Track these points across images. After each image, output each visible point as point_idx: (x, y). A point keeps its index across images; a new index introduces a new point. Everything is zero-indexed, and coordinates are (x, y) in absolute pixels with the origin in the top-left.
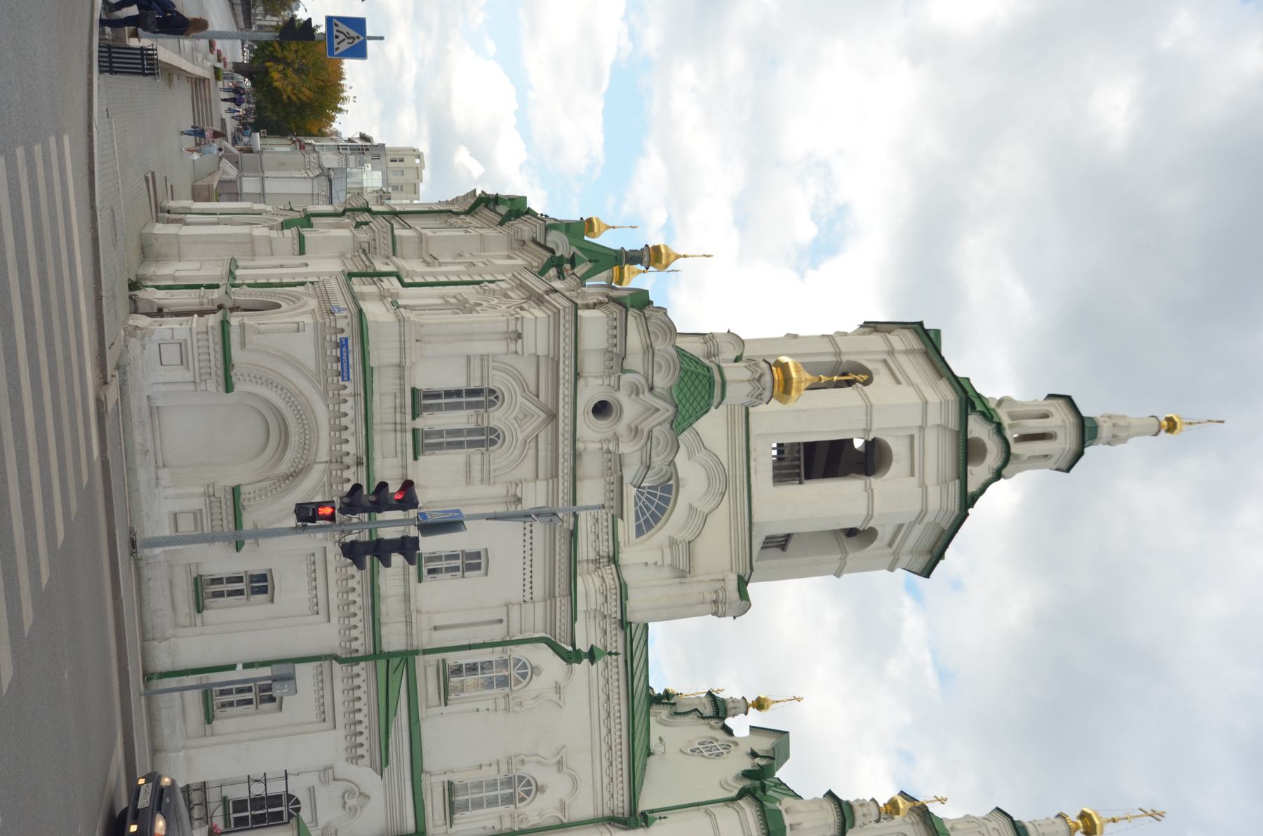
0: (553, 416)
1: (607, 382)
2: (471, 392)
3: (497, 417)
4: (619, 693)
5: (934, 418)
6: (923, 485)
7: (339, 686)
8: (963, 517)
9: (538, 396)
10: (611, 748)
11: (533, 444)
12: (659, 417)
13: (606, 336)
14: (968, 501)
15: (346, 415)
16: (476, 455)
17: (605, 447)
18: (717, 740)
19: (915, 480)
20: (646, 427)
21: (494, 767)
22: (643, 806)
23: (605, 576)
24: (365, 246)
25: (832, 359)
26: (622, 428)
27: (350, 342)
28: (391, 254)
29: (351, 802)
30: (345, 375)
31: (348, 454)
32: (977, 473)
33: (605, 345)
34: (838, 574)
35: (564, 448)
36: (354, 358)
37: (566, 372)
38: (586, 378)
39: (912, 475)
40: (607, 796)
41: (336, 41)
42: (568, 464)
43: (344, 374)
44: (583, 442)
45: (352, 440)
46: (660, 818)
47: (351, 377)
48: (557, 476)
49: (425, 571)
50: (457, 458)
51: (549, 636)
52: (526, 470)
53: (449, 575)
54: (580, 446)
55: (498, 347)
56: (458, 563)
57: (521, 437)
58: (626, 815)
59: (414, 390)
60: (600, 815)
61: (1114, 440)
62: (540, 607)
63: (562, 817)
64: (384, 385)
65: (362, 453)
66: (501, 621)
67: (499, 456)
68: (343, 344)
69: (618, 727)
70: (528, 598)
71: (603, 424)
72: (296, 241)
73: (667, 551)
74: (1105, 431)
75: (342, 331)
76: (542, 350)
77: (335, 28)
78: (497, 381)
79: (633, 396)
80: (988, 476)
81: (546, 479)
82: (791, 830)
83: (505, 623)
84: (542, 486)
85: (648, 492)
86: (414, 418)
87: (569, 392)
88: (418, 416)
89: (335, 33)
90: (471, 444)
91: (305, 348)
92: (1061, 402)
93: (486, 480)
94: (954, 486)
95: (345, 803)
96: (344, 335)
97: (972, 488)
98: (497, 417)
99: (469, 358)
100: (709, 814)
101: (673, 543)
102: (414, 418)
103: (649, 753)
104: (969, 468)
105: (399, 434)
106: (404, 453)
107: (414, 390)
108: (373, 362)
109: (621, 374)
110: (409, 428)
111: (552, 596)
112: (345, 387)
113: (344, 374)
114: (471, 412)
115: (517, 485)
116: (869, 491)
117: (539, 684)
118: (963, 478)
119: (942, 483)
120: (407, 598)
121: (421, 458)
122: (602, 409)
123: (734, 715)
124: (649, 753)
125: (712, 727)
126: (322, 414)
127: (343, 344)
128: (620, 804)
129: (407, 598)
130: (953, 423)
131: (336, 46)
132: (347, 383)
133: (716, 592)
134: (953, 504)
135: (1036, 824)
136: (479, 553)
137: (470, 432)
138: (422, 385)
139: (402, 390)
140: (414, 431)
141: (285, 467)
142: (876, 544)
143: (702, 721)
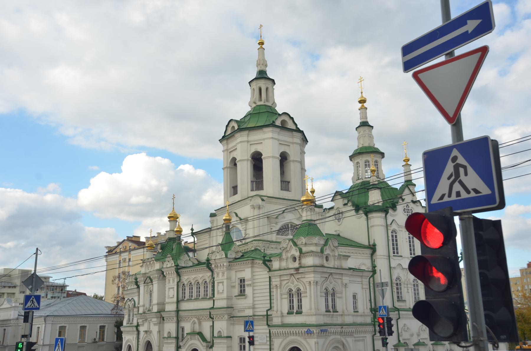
0: (331, 274)
3: (330, 289)
4: (344, 249)
5: (276, 136)
6: (293, 143)
8: (302, 132)
9: (326, 277)
11: (336, 279)
13: (315, 257)
14: (298, 130)
16: (337, 295)
17: (336, 260)
19: (291, 145)
20: (332, 247)
22: (366, 243)
24: (229, 316)
25: (249, 163)
26: (331, 254)
28: (233, 309)
30: (326, 331)
31: (340, 331)
32: (291, 125)
33: (318, 258)
34: (305, 171)
35: (339, 271)
36: (324, 328)
37: (325, 270)
40: (366, 255)
41: (250, 329)
42: (339, 270)
43: (326, 331)
44: (335, 265)
47: (327, 329)
48: (342, 274)
49: (356, 310)
50: (338, 301)
51: (369, 278)
52: (339, 281)
53: (357, 304)
54: (336, 267)
55: (319, 287)
56: (354, 301)
57: (334, 283)
58: (372, 250)
60: (370, 258)
61: (266, 66)
62: (364, 280)
64: (328, 320)
65: (340, 327)
66: (366, 290)
67: (337, 289)
68: (321, 331)
69: (352, 250)
70: (361, 283)
72: (228, 339)
74: (263, 68)
75: (319, 331)
76: (319, 276)
77: (248, 329)
81: (342, 276)
83: (366, 289)
84: (344, 278)
85: (292, 232)
86: (331, 312)
87: (329, 269)
88: (329, 311)
89: (249, 329)
90: (334, 297)
91: (321, 341)
93: (341, 293)
94: (295, 134)
96: (320, 330)
97: (294, 127)
100: (373, 226)
102: (331, 312)
103: (339, 235)
104: (289, 127)
105: (334, 316)
106: (337, 315)
107: (326, 312)
108: (322, 323)
109: (323, 254)
110: (333, 313)
111: (362, 276)
112: (329, 331)
114: (328, 296)
115: (343, 284)
116: (294, 161)
118: (291, 130)
119: (293, 137)
120: (361, 316)
121: (338, 310)
122: (327, 260)
124: (339, 235)
125: (328, 213)
126: (333, 337)
127: (321, 331)
128: (369, 252)
129: (361, 316)
130: (278, 130)
131: (251, 329)
133: (319, 215)
134: (299, 135)
135: (362, 118)
136: (353, 295)
137: (332, 296)
138: (325, 310)
139: (326, 315)
140: (333, 312)
141: (341, 347)
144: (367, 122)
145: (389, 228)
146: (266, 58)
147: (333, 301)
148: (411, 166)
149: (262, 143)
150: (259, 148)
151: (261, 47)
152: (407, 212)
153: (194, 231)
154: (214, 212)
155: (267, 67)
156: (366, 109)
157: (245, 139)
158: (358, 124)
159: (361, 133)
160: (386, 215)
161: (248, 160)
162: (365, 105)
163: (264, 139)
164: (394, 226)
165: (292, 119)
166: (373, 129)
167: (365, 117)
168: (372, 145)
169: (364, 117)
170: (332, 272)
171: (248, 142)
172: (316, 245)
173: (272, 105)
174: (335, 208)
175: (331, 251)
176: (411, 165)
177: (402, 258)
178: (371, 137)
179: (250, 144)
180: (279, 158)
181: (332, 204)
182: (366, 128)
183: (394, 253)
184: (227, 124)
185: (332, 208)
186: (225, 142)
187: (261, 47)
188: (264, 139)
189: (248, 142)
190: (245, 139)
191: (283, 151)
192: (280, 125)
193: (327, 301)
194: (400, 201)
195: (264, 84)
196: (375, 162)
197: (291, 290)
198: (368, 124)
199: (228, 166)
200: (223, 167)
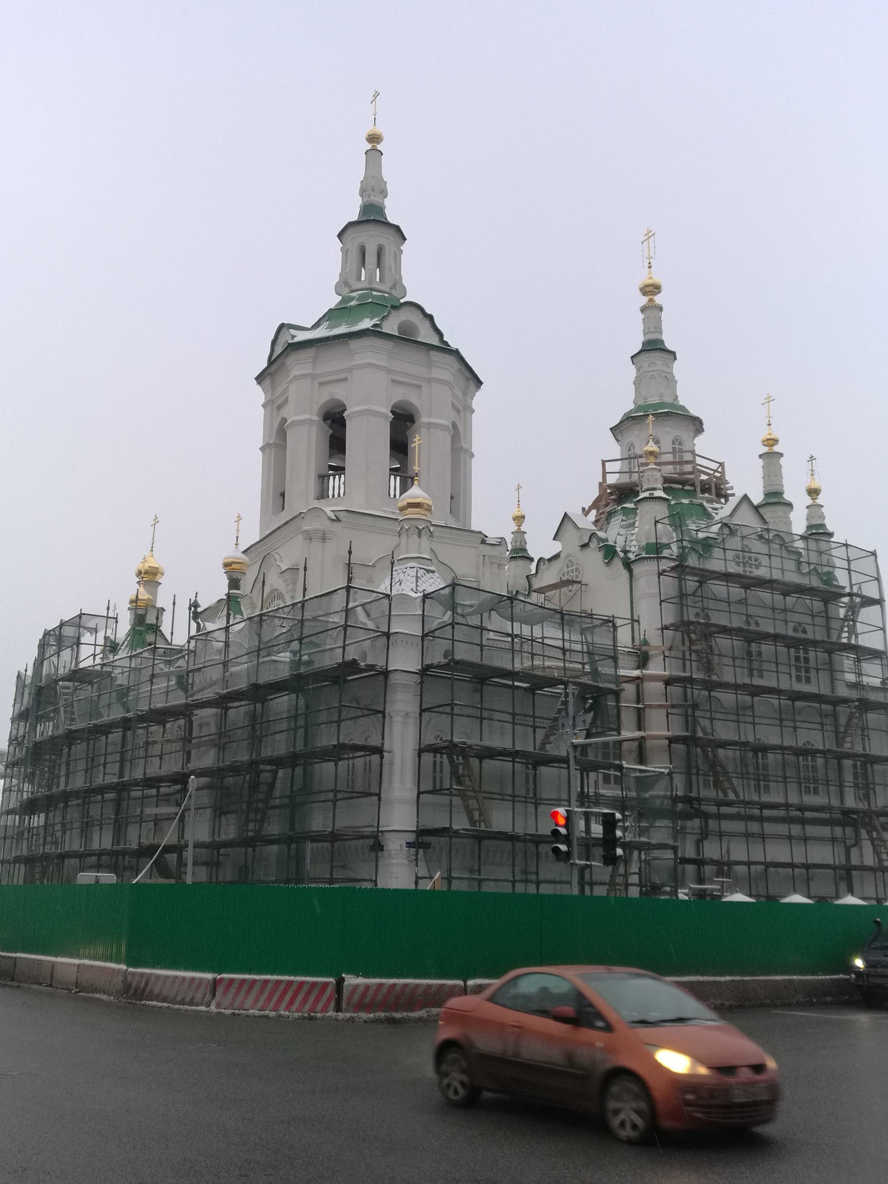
6: (430, 381)
8: (456, 353)
18: (562, 569)
19: (425, 386)
25: (314, 429)
32: (426, 336)
34: (472, 456)
39: (420, 387)
61: (384, 193)
80: (427, 323)
92: (350, 231)
94: (435, 356)
97: (435, 341)
123: (526, 543)
125: (547, 569)
130: (387, 344)
133: (492, 564)
134: (451, 360)
143: (539, 575)
144: (662, 342)
146: (386, 175)
148: (782, 458)
149: (346, 379)
150: (339, 393)
151: (374, 149)
153: (199, 610)
155: (386, 197)
156: (661, 309)
157: (307, 369)
158: (639, 347)
161: (311, 422)
162: (658, 299)
163: (350, 370)
165: (430, 318)
166: (675, 359)
167: (655, 328)
168: (668, 400)
169: (654, 330)
171: (313, 376)
173: (391, 289)
174: (562, 556)
176: (782, 455)
178: (670, 381)
179: (321, 384)
180: (387, 415)
181: (556, 547)
182: (656, 356)
184: (272, 338)
185: (556, 557)
186: (267, 382)
187: (374, 149)
188: (350, 370)
189: (313, 376)
190: (307, 369)
192: (397, 334)
196: (674, 443)
198: (662, 347)
199: (272, 441)
200: (261, 444)
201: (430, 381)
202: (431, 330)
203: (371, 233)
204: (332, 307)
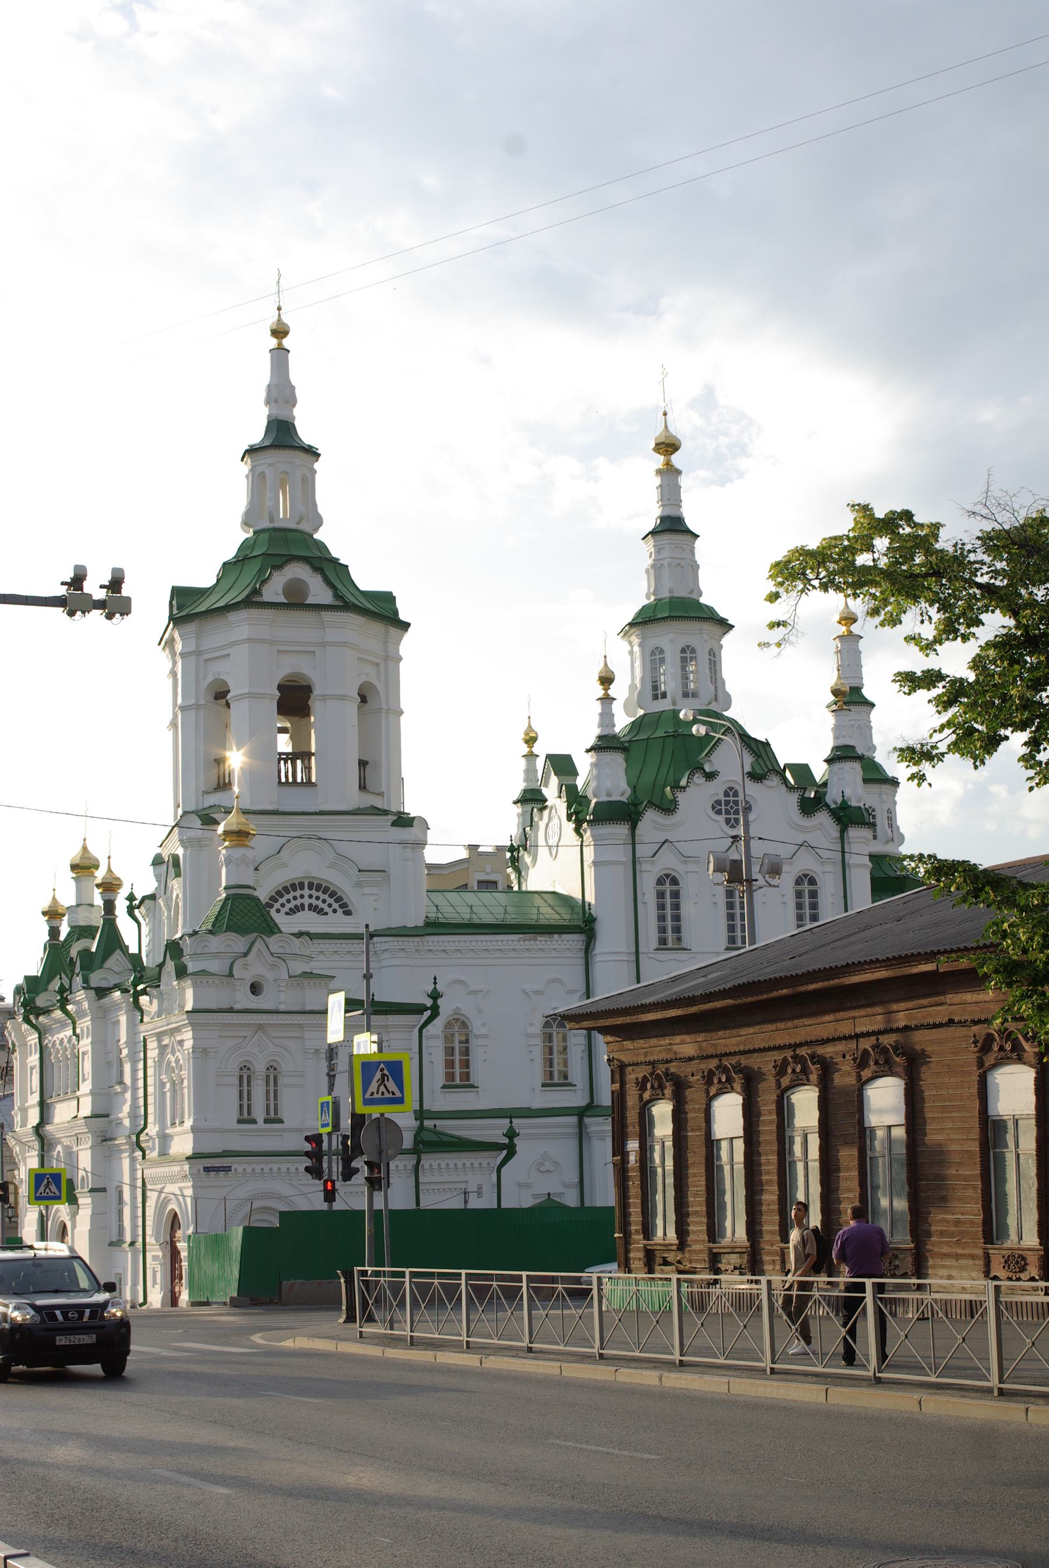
0: (260, 1027)
1: (237, 988)
2: (241, 1084)
3: (259, 1067)
6: (323, 644)
7: (438, 1178)
10: (528, 949)
12: (264, 949)
15: (253, 1169)
21: (531, 1048)
23: (382, 948)
26: (270, 975)
27: (206, 1166)
29: (548, 1166)
38: (235, 1003)
39: (314, 652)
43: (227, 1169)
45: (270, 1165)
46: (590, 909)
59: (239, 1121)
61: (292, 401)
63: (581, 993)
69: (510, 942)
71: (266, 988)
73: (366, 890)
75: (199, 1170)
78: (233, 1066)
79: (248, 967)
82: (611, 796)
94: (327, 615)
95: (548, 1171)
98: (259, 1067)
99: (218, 1085)
101: (359, 885)
107: (239, 1121)
112: (236, 1169)
113: (227, 1169)
117: (468, 1010)
132: (233, 1168)
138: (235, 1116)
142: (375, 681)
145: (645, 867)
147: (273, 1095)
148: (861, 640)
152: (727, 812)
154: (159, 850)
159: (665, 554)
160: (633, 828)
162: (676, 459)
164: (667, 862)
170: (262, 1022)
172: (216, 955)
175: (268, 967)
177: (691, 956)
182: (666, 538)
183: (663, 941)
191: (291, 671)
193: (245, 1096)
194: (698, 779)
195: (270, 465)
197: (245, 1067)
201: (323, 644)
202: (323, 585)
203: (269, 461)
204: (230, 553)
